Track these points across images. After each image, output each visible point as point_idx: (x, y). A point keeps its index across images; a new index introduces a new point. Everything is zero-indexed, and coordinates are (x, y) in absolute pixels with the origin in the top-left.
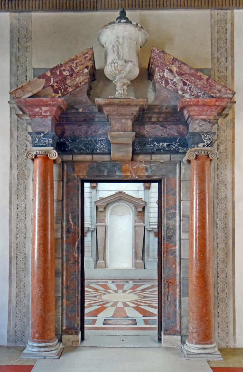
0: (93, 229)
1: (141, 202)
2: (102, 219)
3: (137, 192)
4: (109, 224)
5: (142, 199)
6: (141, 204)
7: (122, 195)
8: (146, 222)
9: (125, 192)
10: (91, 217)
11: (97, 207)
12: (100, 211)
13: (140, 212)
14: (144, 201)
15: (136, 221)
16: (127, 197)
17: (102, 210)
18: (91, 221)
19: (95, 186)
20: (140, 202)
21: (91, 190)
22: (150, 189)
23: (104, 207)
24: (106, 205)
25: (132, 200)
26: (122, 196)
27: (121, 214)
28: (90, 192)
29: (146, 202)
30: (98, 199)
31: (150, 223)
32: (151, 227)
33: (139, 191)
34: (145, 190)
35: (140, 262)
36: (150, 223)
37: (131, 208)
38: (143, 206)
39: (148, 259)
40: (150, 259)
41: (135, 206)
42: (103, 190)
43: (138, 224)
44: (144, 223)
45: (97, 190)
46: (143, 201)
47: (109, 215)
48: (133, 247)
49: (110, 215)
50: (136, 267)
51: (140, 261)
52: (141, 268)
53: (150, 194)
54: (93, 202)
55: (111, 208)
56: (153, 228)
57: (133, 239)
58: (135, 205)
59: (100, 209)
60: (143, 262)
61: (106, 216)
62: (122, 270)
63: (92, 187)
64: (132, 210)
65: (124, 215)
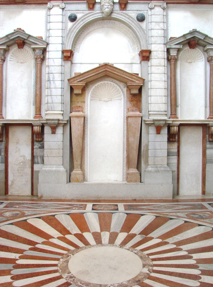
0: (66, 122)
1: (136, 80)
2: (79, 106)
3: (131, 65)
4: (89, 115)
5: (138, 74)
6: (137, 82)
7: (108, 68)
8: (143, 111)
9: (113, 65)
10: (62, 103)
11: (72, 89)
12: (77, 95)
13: (134, 95)
14: (141, 78)
15: (128, 109)
16: (114, 71)
17: (79, 92)
18: (63, 110)
19: (69, 55)
20: (135, 79)
21: (63, 62)
22: (149, 60)
23: (82, 87)
24: (84, 84)
25: (123, 76)
26: (108, 70)
27: (106, 99)
28: (61, 66)
29: (144, 80)
30: (73, 75)
32: (152, 118)
33: (134, 65)
34: (143, 62)
35: (134, 173)
36: (150, 113)
37: (122, 90)
38: (139, 85)
39: (146, 167)
40: (150, 169)
41: (127, 87)
42: (81, 63)
43: (131, 113)
45: (72, 63)
46: (139, 77)
47: (89, 100)
48: (123, 150)
49: (91, 100)
50: (128, 180)
52: (136, 181)
53: (149, 68)
54: (66, 81)
55: (91, 90)
58: (128, 84)
59: (76, 91)
60: (139, 172)
61: (84, 102)
62: (109, 185)
63: (65, 57)
64: (123, 92)
65: (111, 101)
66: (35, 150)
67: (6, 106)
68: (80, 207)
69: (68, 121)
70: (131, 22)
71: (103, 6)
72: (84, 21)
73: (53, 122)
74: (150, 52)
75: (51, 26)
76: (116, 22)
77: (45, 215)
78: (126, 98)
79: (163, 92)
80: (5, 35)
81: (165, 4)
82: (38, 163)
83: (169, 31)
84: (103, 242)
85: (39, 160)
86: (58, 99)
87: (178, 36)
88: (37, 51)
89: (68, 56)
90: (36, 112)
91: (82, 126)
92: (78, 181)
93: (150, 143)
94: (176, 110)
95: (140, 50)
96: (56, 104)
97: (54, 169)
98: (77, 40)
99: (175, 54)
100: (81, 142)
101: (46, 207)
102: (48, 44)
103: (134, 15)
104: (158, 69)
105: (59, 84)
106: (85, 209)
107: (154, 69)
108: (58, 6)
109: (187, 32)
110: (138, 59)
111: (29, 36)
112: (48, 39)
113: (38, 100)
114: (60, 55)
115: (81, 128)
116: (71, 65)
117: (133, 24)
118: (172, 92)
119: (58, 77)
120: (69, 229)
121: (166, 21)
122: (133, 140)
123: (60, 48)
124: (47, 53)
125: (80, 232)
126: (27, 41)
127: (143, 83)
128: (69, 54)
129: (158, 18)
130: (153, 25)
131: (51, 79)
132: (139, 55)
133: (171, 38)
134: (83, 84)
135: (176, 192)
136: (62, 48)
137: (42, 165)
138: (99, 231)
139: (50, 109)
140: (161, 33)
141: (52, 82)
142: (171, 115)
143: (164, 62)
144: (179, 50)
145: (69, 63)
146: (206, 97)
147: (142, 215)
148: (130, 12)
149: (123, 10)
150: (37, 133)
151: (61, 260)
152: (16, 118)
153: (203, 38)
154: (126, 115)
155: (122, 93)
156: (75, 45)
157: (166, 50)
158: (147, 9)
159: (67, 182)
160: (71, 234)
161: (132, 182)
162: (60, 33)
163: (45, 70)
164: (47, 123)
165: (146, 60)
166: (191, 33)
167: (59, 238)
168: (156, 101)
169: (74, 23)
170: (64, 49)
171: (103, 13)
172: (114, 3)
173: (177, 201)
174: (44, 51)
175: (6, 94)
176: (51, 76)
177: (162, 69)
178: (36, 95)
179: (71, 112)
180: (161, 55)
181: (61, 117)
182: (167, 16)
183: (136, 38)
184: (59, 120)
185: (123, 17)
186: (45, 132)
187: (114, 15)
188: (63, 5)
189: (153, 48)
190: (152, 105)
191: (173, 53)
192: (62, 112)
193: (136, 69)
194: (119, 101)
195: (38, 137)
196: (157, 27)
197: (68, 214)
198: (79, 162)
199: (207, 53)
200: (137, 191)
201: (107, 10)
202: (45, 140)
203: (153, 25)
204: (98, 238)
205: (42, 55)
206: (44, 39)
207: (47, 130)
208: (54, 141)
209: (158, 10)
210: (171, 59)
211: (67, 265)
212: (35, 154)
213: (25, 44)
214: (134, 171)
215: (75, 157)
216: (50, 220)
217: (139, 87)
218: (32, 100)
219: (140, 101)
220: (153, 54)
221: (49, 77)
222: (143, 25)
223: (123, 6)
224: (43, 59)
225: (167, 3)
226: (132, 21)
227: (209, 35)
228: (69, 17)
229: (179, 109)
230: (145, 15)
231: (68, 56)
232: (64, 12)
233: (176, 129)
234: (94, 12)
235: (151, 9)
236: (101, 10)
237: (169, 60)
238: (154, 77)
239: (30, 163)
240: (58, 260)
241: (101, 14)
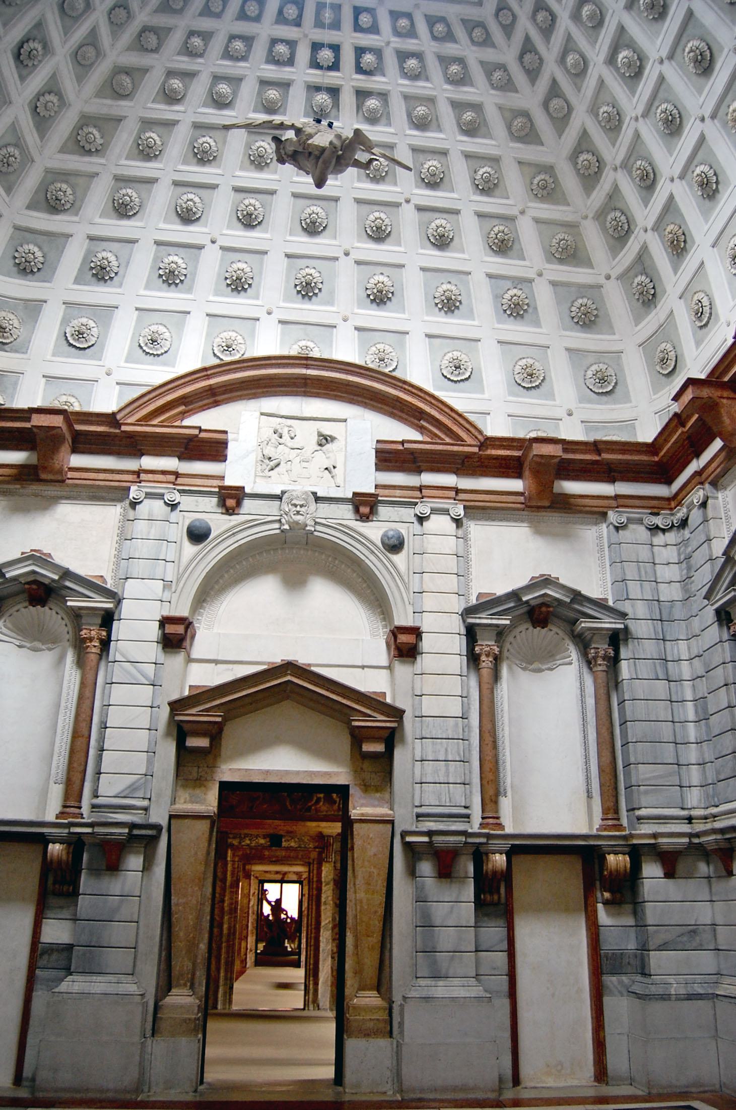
44: (392, 809)
89: (175, 636)
95: (388, 630)
102: (119, 602)
107: (429, 684)
111: (67, 574)
114: (153, 631)
142: (483, 818)
143: (458, 663)
145: (178, 659)
153: (568, 600)
157: (463, 631)
174: (108, 619)
182: (465, 538)
189: (427, 623)
209: (440, 524)
210: (479, 655)
213: (53, 595)
217: (385, 734)
222: (399, 559)
225: (465, 507)
231: (175, 636)
237: (473, 659)
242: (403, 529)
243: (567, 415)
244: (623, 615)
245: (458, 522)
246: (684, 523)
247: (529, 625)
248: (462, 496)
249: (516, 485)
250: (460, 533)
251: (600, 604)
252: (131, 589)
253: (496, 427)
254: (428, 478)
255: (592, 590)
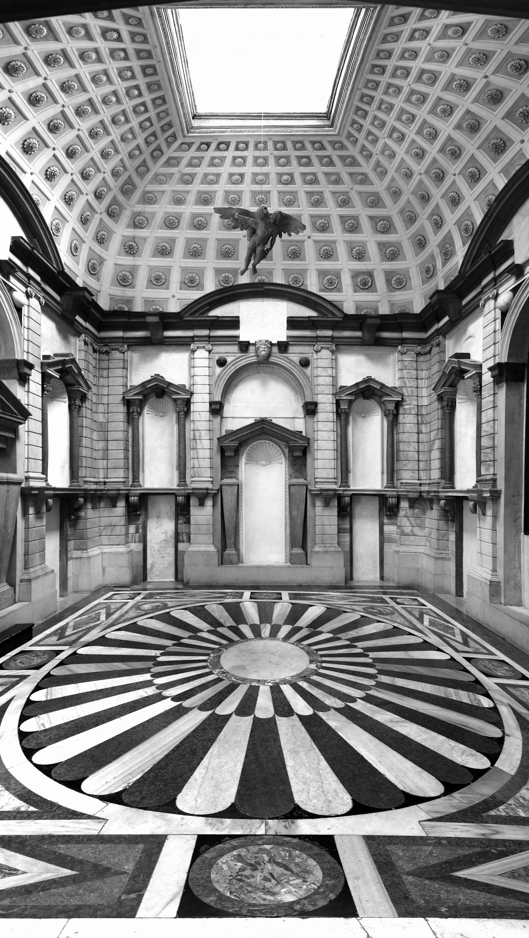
1: (300, 439)
4: (243, 482)
5: (301, 432)
8: (308, 478)
11: (222, 450)
13: (297, 458)
15: (290, 475)
20: (298, 438)
29: (308, 440)
30: (224, 433)
31: (317, 480)
32: (319, 486)
34: (307, 417)
36: (317, 480)
37: (283, 451)
40: (317, 549)
41: (289, 447)
42: (233, 418)
43: (294, 481)
45: (222, 417)
46: (303, 436)
47: (243, 463)
49: (245, 464)
51: (299, 552)
52: (301, 564)
54: (216, 441)
55: (246, 451)
56: (322, 490)
57: (286, 509)
59: (227, 454)
61: (238, 466)
64: (284, 454)
65: (270, 464)
66: (179, 526)
67: (143, 471)
68: (235, 596)
69: (218, 490)
70: (292, 367)
71: (258, 348)
72: (236, 366)
73: (201, 491)
74: (316, 404)
75: (197, 371)
76: (275, 367)
77: (192, 605)
78: (287, 462)
79: (331, 445)
80: (140, 383)
81: (334, 345)
82: (183, 542)
83: (339, 378)
84: (263, 636)
85: (185, 538)
86: (206, 463)
87: (349, 384)
88: (180, 402)
89: (216, 409)
90: (180, 479)
91: (236, 497)
92: (231, 563)
93: (317, 518)
94: (347, 478)
96: (204, 468)
97: (203, 549)
98: (228, 388)
99: (346, 407)
100: (234, 516)
101: (193, 596)
102: (192, 394)
103: (296, 359)
104: (326, 425)
105: (206, 444)
106: (241, 598)
107: (321, 426)
108: (204, 347)
109: (360, 380)
110: (301, 413)
111: (170, 384)
112: (192, 388)
113: (182, 464)
114: (207, 407)
115: (234, 498)
116: (221, 420)
117: (295, 369)
118: (343, 455)
119: (205, 435)
120: (222, 621)
121: (335, 366)
122: (296, 513)
123: (207, 398)
124: (192, 405)
125: (234, 624)
126: (167, 390)
127: (309, 443)
128: (218, 407)
129: (325, 363)
130: (320, 372)
131: (197, 438)
132: (303, 407)
133: (341, 387)
134: (235, 444)
135: (350, 576)
136: (210, 398)
137: (188, 544)
138: (257, 622)
139: (197, 475)
140: (329, 380)
141: (198, 441)
143: (332, 416)
144: (350, 402)
145: (218, 419)
146: (383, 461)
147: (311, 606)
148: (291, 355)
149: (283, 353)
150: (182, 504)
151: (212, 655)
152: (156, 486)
153: (379, 388)
154: (288, 483)
155: (282, 455)
156: (225, 394)
157: (335, 402)
158: (312, 351)
159: (219, 565)
160: (224, 626)
161: (296, 564)
162: (206, 381)
163: (189, 427)
164: (193, 493)
165: (312, 414)
166: (365, 381)
167: (209, 631)
168: (323, 465)
169: (223, 368)
170: (212, 400)
171: (258, 356)
172: (272, 345)
173: (351, 588)
174: (188, 403)
175: (143, 456)
176: (197, 433)
177: (330, 426)
178: (179, 458)
179: (222, 479)
180: (329, 408)
181: (210, 486)
182: (336, 359)
183: (298, 388)
184: (207, 489)
185: (284, 362)
186: (191, 504)
187: (272, 359)
188: (210, 347)
189: (320, 399)
190: (319, 470)
191: (344, 406)
192: (211, 479)
193: (299, 425)
194: (280, 465)
195: (182, 512)
196: (324, 373)
197: (221, 604)
198: (232, 541)
199: (384, 405)
200: (302, 575)
201: (263, 353)
202: (191, 514)
203: (320, 372)
204: (256, 631)
205: (185, 409)
206: (187, 388)
207: (193, 501)
208: (202, 515)
209: (325, 353)
211: (219, 660)
212: (179, 531)
214: (298, 551)
215: (228, 536)
216: (199, 610)
218: (175, 463)
219: (305, 465)
220: (320, 407)
221: (194, 435)
222: (308, 371)
223: (283, 349)
224: (188, 413)
225: (336, 345)
226: (295, 367)
227: (386, 384)
228: (217, 361)
229: (351, 476)
230: (310, 358)
231: (216, 409)
232: (211, 354)
233: (347, 499)
234: (248, 355)
235: (317, 352)
236: (256, 353)
238: (320, 435)
239: (173, 541)
240: (208, 655)
241: (255, 358)
242: (309, 356)
243: (382, 301)
244: (402, 395)
245: (333, 352)
246: (430, 352)
247: (362, 399)
248: (335, 340)
249: (359, 334)
250: (334, 357)
251: (393, 389)
252: (197, 389)
253: (350, 309)
254: (320, 333)
255: (390, 384)
